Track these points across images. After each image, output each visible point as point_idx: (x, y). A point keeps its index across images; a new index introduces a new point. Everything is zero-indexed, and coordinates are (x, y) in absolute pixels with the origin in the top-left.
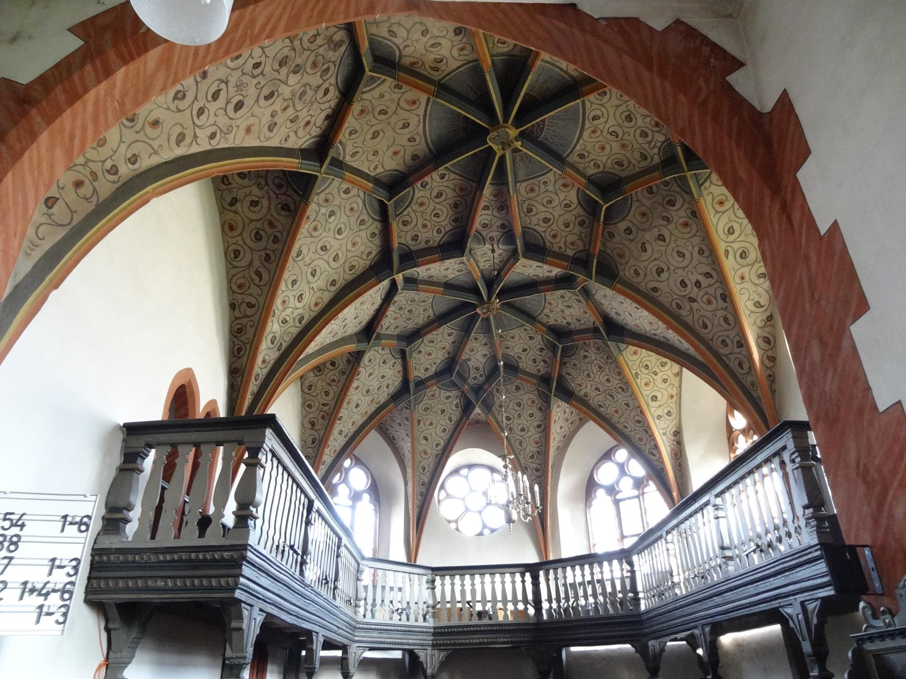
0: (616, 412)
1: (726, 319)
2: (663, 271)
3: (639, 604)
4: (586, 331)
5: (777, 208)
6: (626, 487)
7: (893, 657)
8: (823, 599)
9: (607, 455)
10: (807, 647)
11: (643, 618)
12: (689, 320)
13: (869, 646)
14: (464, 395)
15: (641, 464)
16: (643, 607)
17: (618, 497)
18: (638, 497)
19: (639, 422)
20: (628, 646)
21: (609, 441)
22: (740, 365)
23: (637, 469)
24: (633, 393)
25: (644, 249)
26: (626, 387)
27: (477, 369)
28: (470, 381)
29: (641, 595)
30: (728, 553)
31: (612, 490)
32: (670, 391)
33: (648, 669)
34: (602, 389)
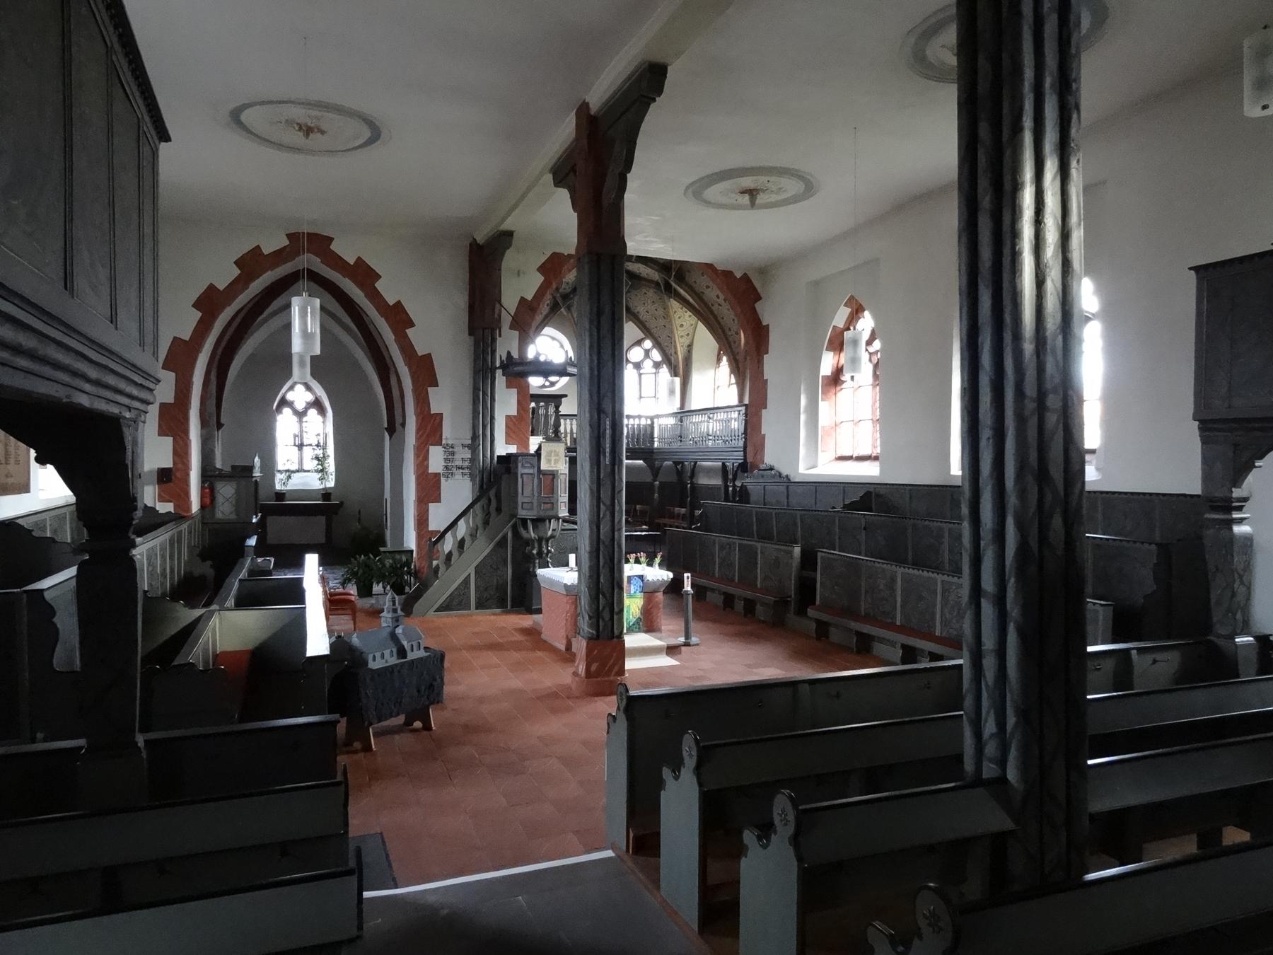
0: (656, 327)
1: (733, 320)
2: (709, 287)
3: (654, 444)
4: (651, 281)
5: (756, 361)
6: (648, 365)
7: (748, 487)
8: (740, 464)
9: (639, 343)
10: (730, 477)
11: (655, 451)
12: (716, 313)
13: (745, 484)
14: (554, 298)
15: (659, 353)
16: (656, 445)
17: (641, 371)
18: (655, 373)
19: (669, 337)
20: (641, 461)
21: (641, 335)
22: (735, 342)
23: (656, 356)
24: (671, 321)
25: (703, 274)
26: (667, 316)
27: (568, 283)
28: (561, 290)
29: (656, 439)
30: (710, 438)
31: (638, 366)
32: (692, 322)
33: (653, 475)
34: (649, 311)
